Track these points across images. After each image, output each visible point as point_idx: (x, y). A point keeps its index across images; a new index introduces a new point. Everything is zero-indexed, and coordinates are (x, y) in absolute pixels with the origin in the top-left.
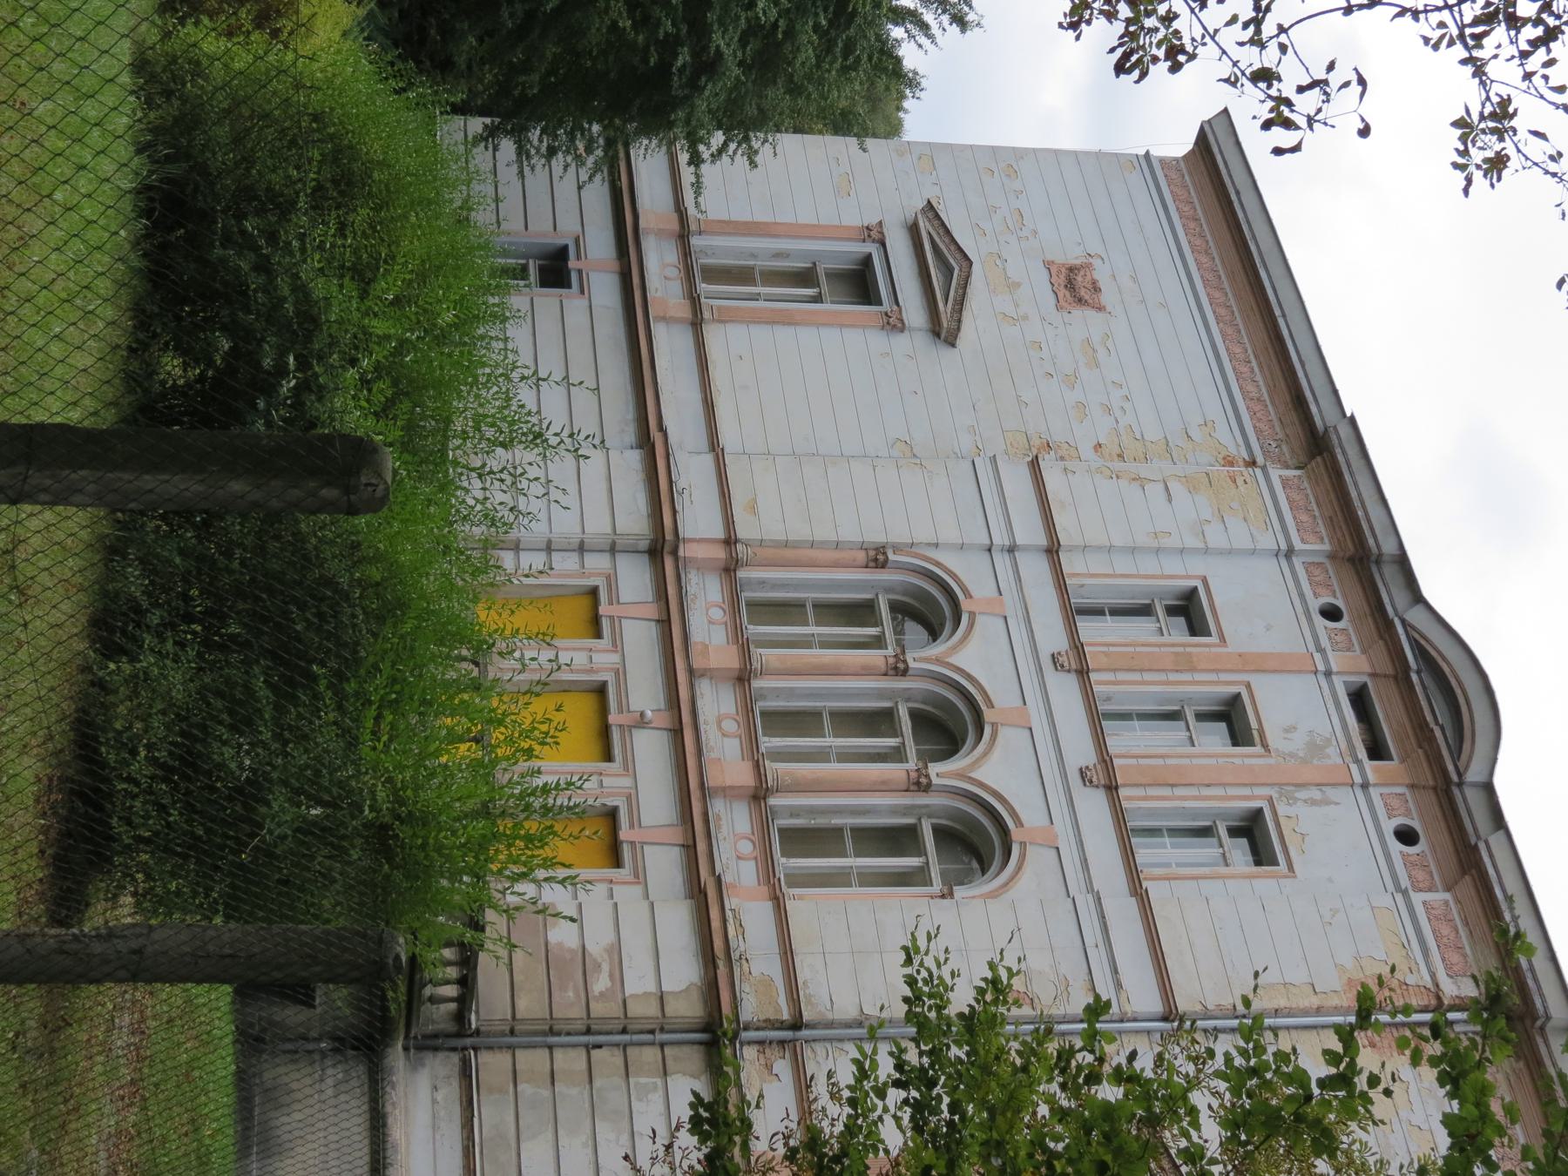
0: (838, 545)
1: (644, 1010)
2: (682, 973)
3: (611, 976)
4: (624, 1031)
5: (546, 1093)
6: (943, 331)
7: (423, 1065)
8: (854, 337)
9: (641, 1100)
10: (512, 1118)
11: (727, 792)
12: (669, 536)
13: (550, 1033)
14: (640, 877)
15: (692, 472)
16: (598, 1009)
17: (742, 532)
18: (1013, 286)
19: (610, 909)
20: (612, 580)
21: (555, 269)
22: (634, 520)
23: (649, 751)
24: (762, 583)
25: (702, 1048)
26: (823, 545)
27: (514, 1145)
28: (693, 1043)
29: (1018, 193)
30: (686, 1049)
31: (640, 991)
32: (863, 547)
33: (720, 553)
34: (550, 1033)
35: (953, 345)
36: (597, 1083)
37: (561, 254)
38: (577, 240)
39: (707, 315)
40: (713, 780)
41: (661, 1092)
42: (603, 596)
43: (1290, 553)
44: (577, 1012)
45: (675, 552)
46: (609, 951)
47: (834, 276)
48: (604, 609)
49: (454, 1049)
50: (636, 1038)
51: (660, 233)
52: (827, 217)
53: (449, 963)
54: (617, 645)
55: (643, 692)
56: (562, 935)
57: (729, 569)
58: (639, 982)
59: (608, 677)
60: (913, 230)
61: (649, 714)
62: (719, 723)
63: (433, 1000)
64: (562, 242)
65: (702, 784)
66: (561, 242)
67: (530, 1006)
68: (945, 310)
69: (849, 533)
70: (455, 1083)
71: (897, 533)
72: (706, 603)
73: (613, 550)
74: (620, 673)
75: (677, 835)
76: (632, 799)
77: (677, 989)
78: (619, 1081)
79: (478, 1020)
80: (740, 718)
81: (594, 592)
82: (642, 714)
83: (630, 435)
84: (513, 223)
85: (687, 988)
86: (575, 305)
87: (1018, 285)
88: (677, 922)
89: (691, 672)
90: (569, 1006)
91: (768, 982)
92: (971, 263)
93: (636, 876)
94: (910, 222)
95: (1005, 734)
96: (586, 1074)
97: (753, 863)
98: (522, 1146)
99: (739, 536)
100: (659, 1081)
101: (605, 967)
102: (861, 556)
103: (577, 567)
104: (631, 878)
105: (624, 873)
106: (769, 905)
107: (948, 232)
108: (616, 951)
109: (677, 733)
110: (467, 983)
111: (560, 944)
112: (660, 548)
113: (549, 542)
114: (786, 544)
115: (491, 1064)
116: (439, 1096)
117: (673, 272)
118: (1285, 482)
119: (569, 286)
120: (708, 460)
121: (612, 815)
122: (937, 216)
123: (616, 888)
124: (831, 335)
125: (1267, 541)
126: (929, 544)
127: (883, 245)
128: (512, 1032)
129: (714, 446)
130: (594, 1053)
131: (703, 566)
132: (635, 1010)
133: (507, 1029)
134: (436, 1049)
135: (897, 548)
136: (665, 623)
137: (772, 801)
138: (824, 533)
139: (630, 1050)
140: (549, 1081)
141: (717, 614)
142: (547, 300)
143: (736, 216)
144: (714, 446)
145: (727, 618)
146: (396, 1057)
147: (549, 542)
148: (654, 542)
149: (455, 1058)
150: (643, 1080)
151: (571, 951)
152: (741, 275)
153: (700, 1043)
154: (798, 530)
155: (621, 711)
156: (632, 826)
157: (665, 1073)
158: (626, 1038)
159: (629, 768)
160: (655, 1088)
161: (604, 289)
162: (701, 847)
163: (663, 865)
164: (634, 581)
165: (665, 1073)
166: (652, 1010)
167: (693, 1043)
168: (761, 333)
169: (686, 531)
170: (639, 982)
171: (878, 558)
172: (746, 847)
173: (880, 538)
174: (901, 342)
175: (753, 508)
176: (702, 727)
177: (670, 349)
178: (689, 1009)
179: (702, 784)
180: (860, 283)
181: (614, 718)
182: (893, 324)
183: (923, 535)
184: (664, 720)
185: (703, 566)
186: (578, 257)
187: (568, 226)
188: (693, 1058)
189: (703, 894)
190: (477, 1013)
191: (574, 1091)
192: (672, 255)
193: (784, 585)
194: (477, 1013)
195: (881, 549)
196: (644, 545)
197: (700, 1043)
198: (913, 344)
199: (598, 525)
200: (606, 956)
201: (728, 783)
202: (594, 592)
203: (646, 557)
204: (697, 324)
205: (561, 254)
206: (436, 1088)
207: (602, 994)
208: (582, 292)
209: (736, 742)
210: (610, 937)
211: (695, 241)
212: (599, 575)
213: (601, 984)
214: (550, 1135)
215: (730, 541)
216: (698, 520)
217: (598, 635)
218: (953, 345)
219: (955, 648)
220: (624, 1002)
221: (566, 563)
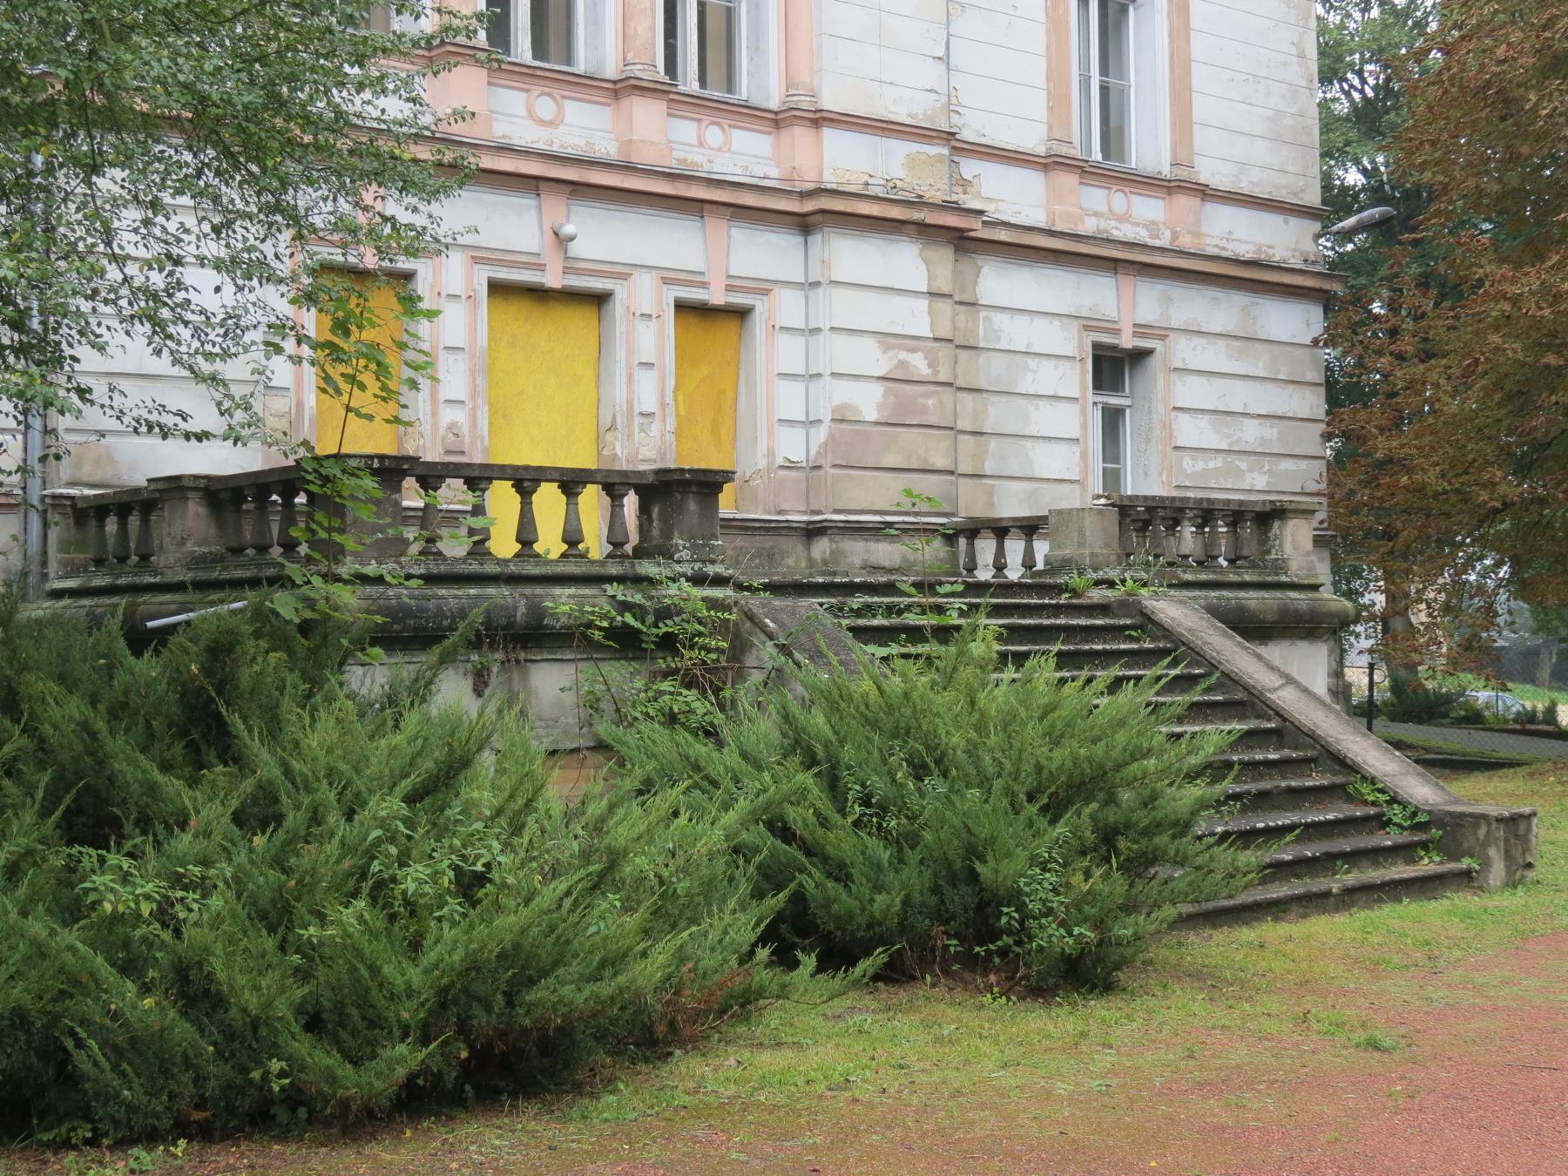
2: (907, 263)
3: (913, 350)
5: (993, 443)
9: (999, 339)
10: (1014, 485)
19: (838, 337)
27: (1035, 485)
31: (927, 320)
36: (984, 385)
46: (887, 348)
53: (1000, 552)
58: (916, 318)
59: (482, 275)
75: (716, 226)
76: (669, 279)
78: (984, 356)
80: (536, 90)
88: (849, 255)
91: (912, 162)
96: (976, 395)
98: (1038, 475)
100: (983, 314)
101: (903, 355)
105: (760, 305)
106: (828, 133)
108: (888, 339)
111: (879, 407)
140: (979, 438)
151: (885, 395)
155: (541, 267)
156: (704, 285)
157: (974, 304)
160: (987, 319)
162: (749, 199)
163: (759, 254)
165: (974, 304)
170: (916, 318)
172: (714, 135)
176: (556, 148)
181: (553, 279)
189: (811, 216)
191: (992, 411)
200: (891, 353)
207: (930, 365)
209: (569, 106)
210: (871, 344)
213: (920, 365)
214: (1029, 444)
220: (936, 339)
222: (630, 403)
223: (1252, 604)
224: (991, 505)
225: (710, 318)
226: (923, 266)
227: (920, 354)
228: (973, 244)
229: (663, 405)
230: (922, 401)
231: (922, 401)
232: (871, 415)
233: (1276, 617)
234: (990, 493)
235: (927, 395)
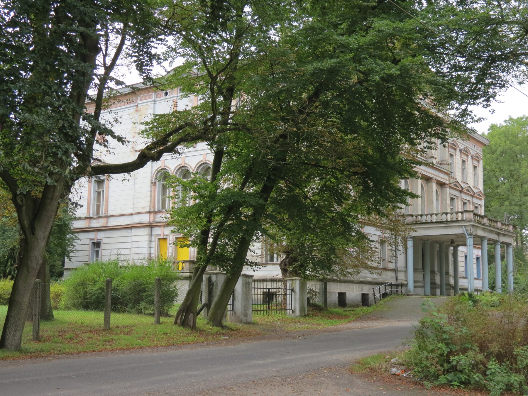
0: (151, 191)
15: (136, 219)
17: (148, 210)
20: (157, 236)
21: (97, 244)
22: (145, 231)
24: (158, 206)
26: (151, 194)
32: (151, 187)
33: (152, 214)
37: (94, 243)
42: (159, 237)
43: (154, 101)
45: (152, 223)
47: (98, 188)
48: (162, 237)
51: (90, 223)
57: (155, 213)
66: (91, 243)
69: (149, 189)
71: (149, 179)
73: (151, 235)
81: (159, 239)
83: (129, 231)
84: (87, 253)
95: (186, 162)
102: (153, 187)
112: (151, 226)
114: (151, 202)
117: (97, 221)
118: (141, 100)
120: (134, 216)
124: (111, 190)
125: (152, 105)
129: (132, 214)
131: (154, 218)
135: (152, 180)
138: (149, 194)
142: (103, 246)
144: (132, 214)
152: (98, 206)
154: (148, 199)
161: (101, 235)
164: (157, 231)
168: (110, 204)
169: (147, 221)
171: (154, 184)
173: (150, 183)
175: (144, 208)
177: (113, 222)
183: (149, 175)
185: (154, 218)
187: (87, 242)
192: (94, 221)
193: (159, 202)
195: (152, 183)
196: (150, 229)
199: (146, 238)
202: (159, 239)
204: (108, 217)
205: (94, 243)
211: (91, 216)
215: (150, 213)
216: (145, 219)
217: (167, 238)
219: (171, 170)
221: (153, 244)
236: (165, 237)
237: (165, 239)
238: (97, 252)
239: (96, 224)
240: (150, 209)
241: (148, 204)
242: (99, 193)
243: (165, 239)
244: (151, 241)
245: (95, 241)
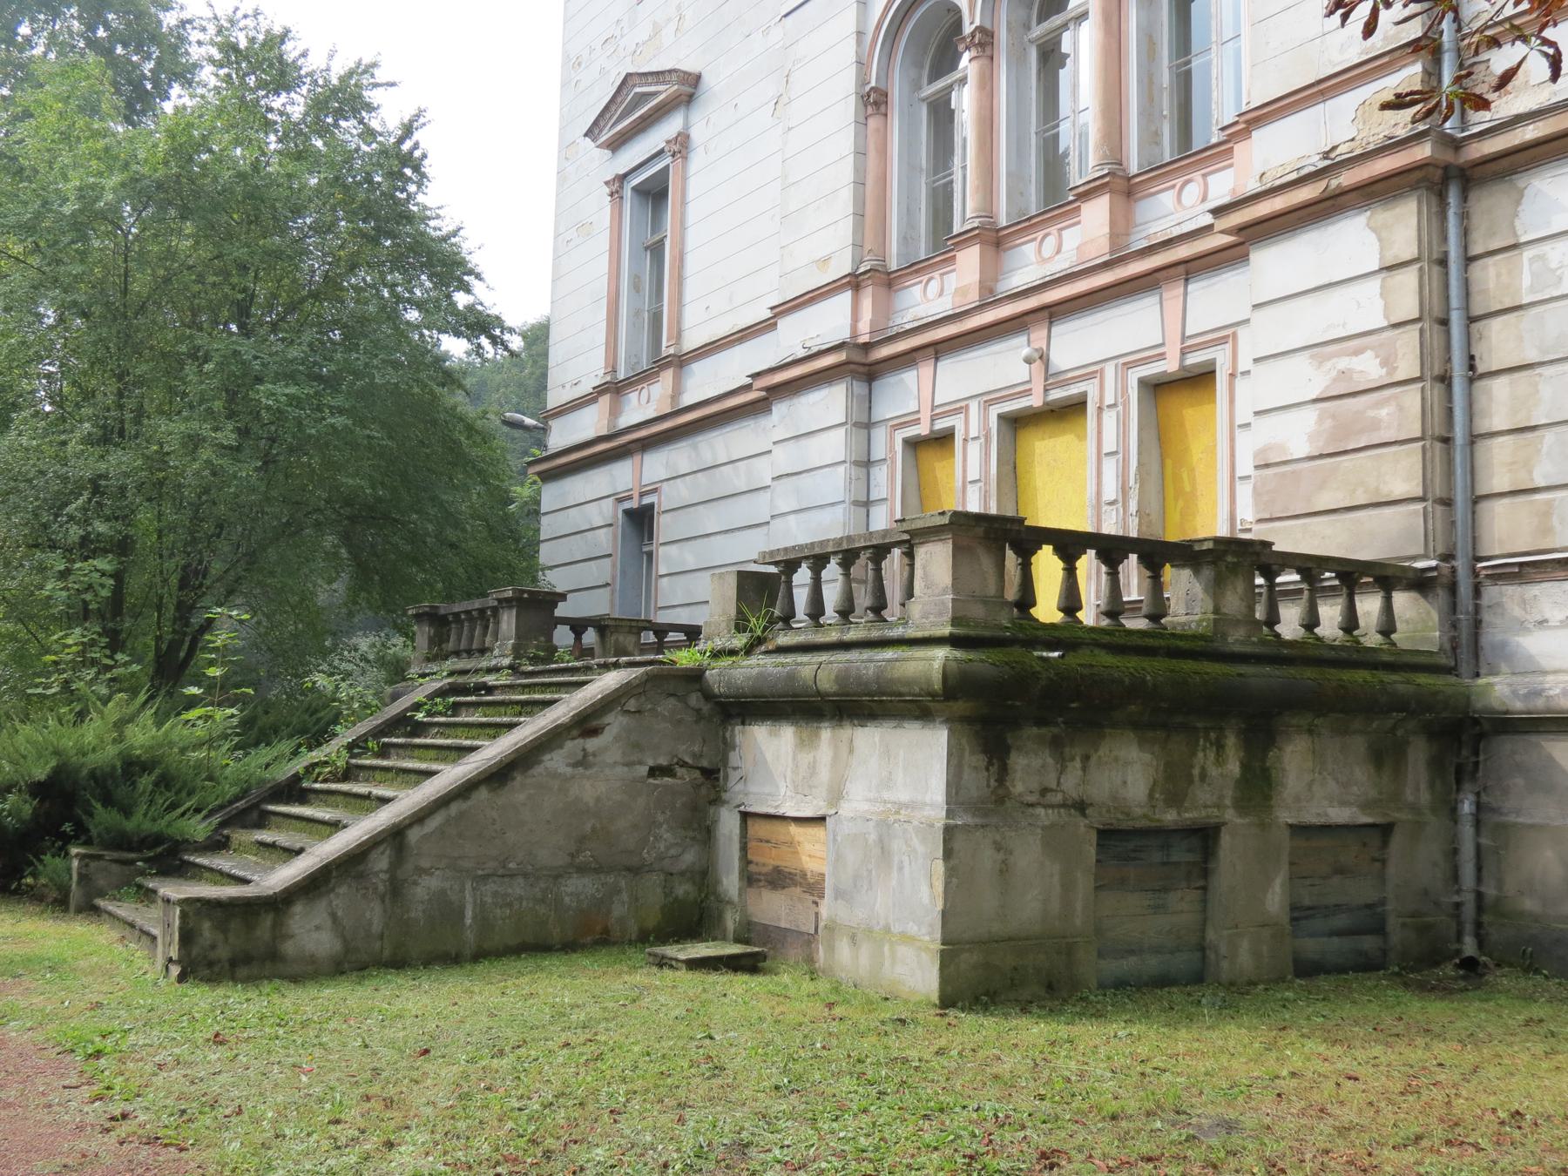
0: (860, 153)
1: (1407, 293)
2: (1354, 241)
3: (1357, 352)
4: (1444, 322)
5: (1549, 436)
6: (687, 90)
7: (1504, 645)
8: (695, 187)
11: (1120, 228)
12: (841, 357)
13: (1451, 440)
14: (1225, 336)
16: (1408, 366)
17: (843, 266)
18: (657, 30)
21: (641, 520)
22: (829, 404)
23: (1078, 344)
24: (905, 240)
25: (1473, 196)
28: (1464, 216)
29: (592, 50)
30: (1479, 222)
31: (1380, 303)
32: (861, 123)
34: (1451, 440)
35: (698, 77)
36: (1532, 356)
38: (620, 500)
39: (672, 351)
40: (1100, 249)
41: (1545, 248)
42: (911, 432)
44: (1412, 399)
45: (867, 347)
49: (1477, 591)
50: (1455, 302)
51: (615, 412)
52: (603, 242)
54: (959, 408)
55: (1002, 368)
56: (1297, 435)
58: (1366, 307)
60: (616, 144)
61: (1026, 351)
62: (1044, 261)
63: (1388, 628)
64: (620, 515)
65: (1107, 265)
67: (1401, 474)
68: (665, 91)
69: (844, 142)
70: (1534, 590)
71: (846, 84)
72: (929, 300)
74: (989, 399)
75: (1173, 293)
77: (1377, 245)
79: (1425, 556)
80: (1040, 235)
82: (1028, 361)
83: (764, 422)
85: (1374, 230)
86: (664, 500)
87: (655, 23)
88: (1279, 265)
89: (981, 307)
90: (1403, 413)
92: (629, 75)
93: (1223, 341)
94: (608, 153)
97: (1210, 179)
99: (848, 270)
101: (1343, 363)
102: (873, 123)
103: (884, 468)
104: (1228, 347)
105: (1221, 357)
107: (607, 108)
109: (1054, 313)
110: (1352, 576)
112: (863, 366)
113: (856, 503)
114: (859, 215)
115: (1507, 531)
116: (1555, 616)
119: (652, 506)
120: (783, 323)
121: (1156, 388)
122: (596, 123)
123: (1241, 368)
124: (694, 212)
126: (859, 42)
127: (625, 176)
128: (1447, 502)
130: (1481, 368)
131: (884, 310)
132: (1408, 306)
133: (1439, 509)
134: (1477, 624)
135: (862, 80)
136: (939, 350)
137: (1134, 169)
139: (1477, 310)
140: (1529, 435)
141: (934, 286)
142: (665, 526)
143: (601, 337)
145: (936, 274)
146: (1500, 690)
147: (856, 503)
148: (855, 375)
149: (1491, 592)
150: (1526, 280)
151: (1320, 420)
153: (1464, 198)
155: (1028, 393)
157: (1515, 246)
158: (1456, 318)
159: (1092, 372)
160: (1541, 258)
161: (656, 465)
163: (1211, 302)
165: (1515, 246)
166: (1408, 280)
167: (1464, 216)
168: (691, 290)
169: (845, 335)
171: (874, 101)
174: (696, 134)
175: (826, 260)
178: (1401, 226)
179: (1107, 265)
180: (655, 194)
181: (1035, 401)
182: (681, 146)
183: (849, 52)
184: (1038, 335)
185: (884, 310)
186: (630, 498)
188: (1488, 203)
190: (1415, 558)
191: (1546, 391)
193: (909, 213)
194: (1415, 558)
196: (860, 388)
197: (1464, 198)
198: (703, 124)
199: (835, 445)
200: (1329, 365)
201: (1107, 230)
203: (875, 384)
206: (1542, 623)
207: (1384, 364)
208: (655, 490)
210: (1301, 362)
212: (892, 438)
213: (1368, 368)
215: (854, 282)
216: (831, 323)
218: (698, 77)
222: (1099, 493)
223: (806, 672)
224: (1547, 530)
225: (1180, 387)
226: (1372, 238)
227: (1369, 354)
228: (1505, 162)
229: (1124, 490)
230: (1371, 413)
231: (1371, 413)
232: (1301, 449)
233: (835, 688)
234: (1546, 512)
235: (1378, 405)
236: (941, 424)
237: (943, 440)
238: (650, 555)
239: (640, 407)
240: (858, 261)
241: (845, 230)
242: (656, 250)
243: (943, 440)
244: (866, 464)
245: (633, 504)
